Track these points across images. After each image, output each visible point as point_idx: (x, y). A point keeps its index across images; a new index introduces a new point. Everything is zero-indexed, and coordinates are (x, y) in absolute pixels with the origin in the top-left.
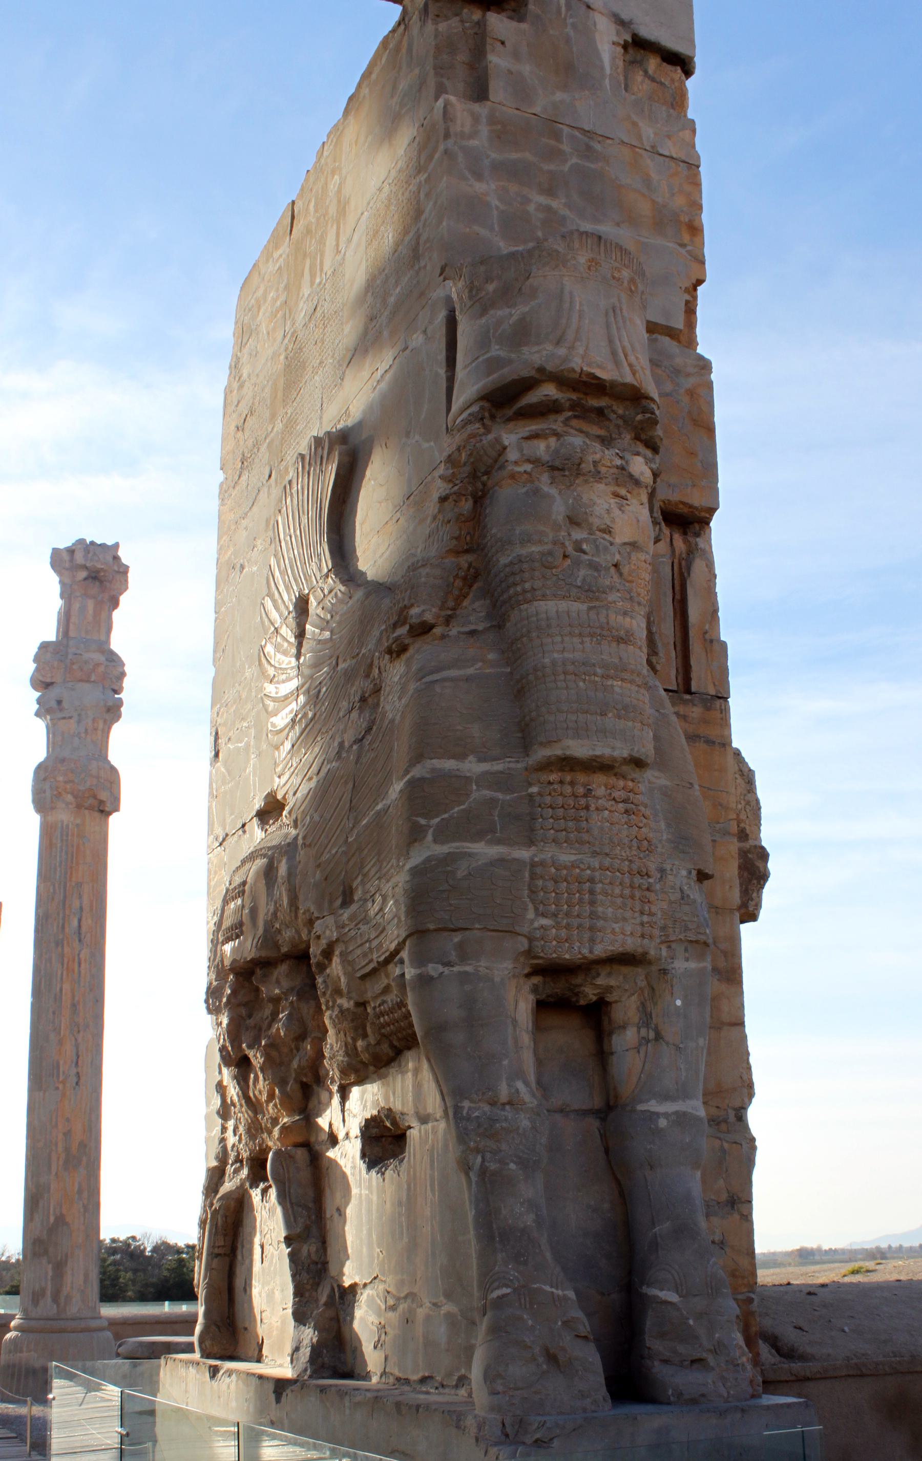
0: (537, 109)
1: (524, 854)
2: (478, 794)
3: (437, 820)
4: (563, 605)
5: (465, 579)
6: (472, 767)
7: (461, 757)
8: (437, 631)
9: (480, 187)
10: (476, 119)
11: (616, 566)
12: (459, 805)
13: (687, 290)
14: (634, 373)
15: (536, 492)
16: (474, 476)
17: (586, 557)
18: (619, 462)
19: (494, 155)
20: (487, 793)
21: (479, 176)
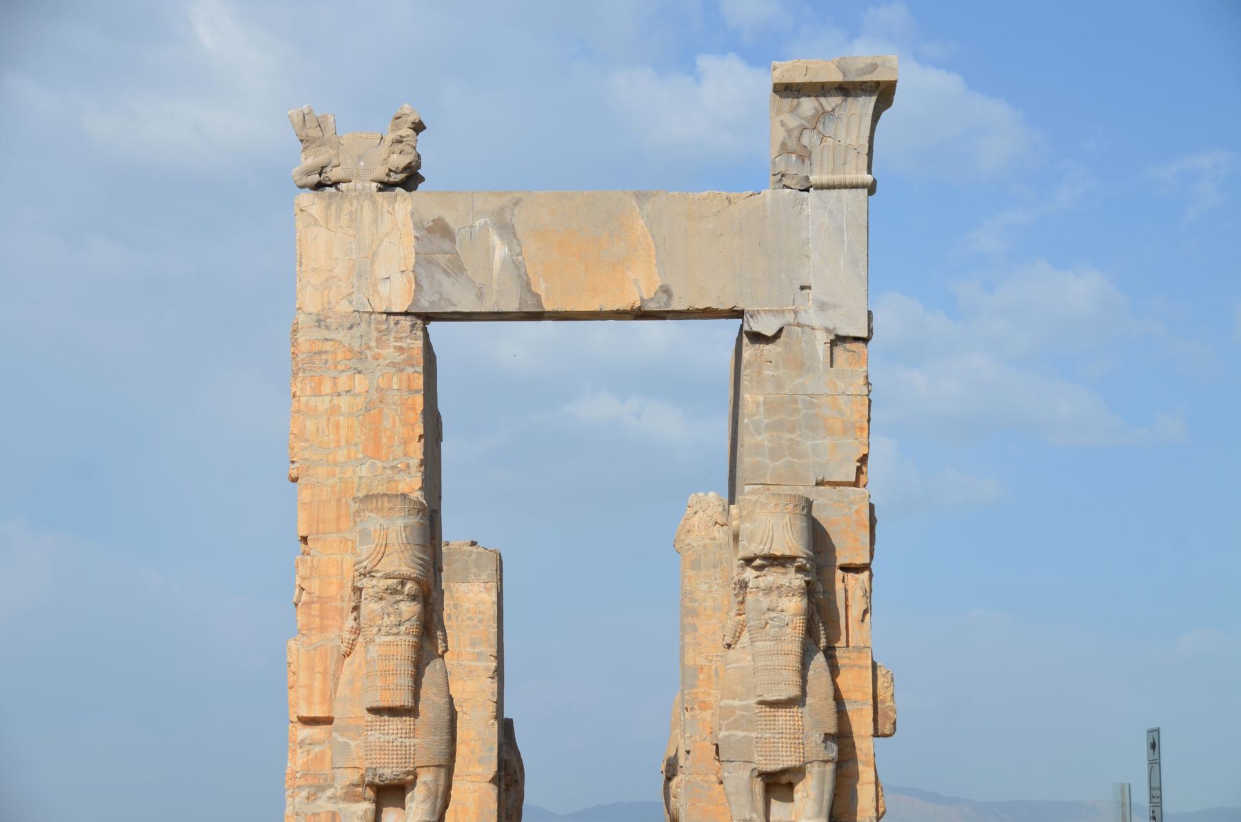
0: (787, 391)
1: (754, 735)
2: (738, 713)
3: (725, 723)
4: (765, 643)
5: (742, 625)
6: (737, 703)
7: (734, 699)
8: (732, 646)
9: (759, 438)
10: (758, 404)
11: (787, 624)
13: (858, 461)
14: (791, 550)
15: (757, 600)
16: (741, 587)
17: (776, 623)
18: (787, 584)
19: (766, 421)
20: (742, 713)
21: (759, 433)
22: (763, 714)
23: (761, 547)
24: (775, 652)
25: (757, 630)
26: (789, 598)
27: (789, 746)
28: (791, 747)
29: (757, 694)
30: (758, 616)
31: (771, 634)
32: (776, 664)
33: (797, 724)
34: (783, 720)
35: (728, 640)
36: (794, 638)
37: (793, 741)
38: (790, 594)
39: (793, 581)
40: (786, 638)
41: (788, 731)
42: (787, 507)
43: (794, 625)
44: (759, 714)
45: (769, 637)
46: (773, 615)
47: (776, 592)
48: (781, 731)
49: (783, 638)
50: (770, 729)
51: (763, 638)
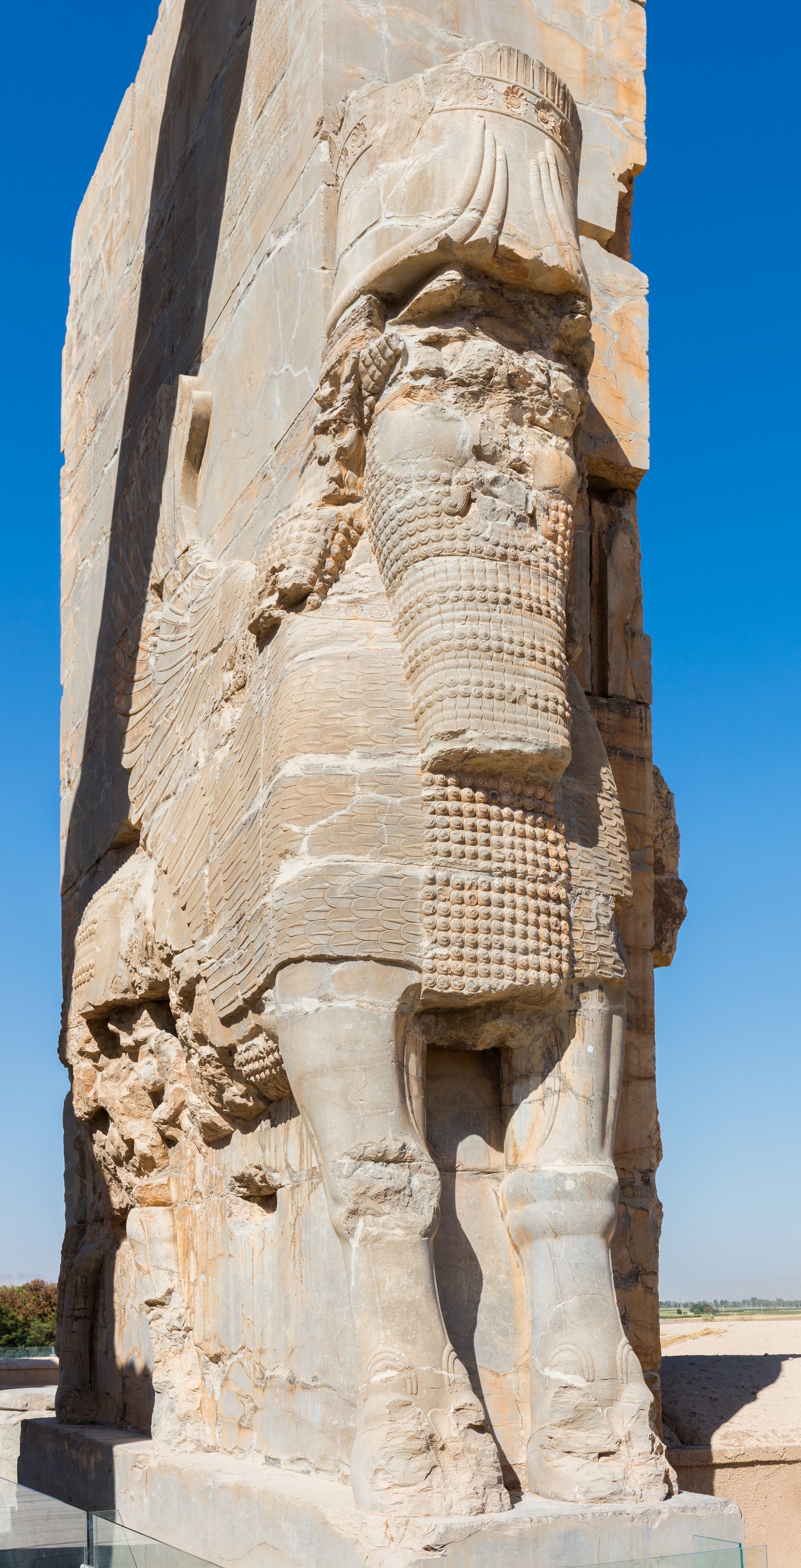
12: (339, 810)
16: (357, 398)
18: (540, 378)
20: (372, 795)
22: (452, 805)
23: (469, 216)
24: (502, 596)
25: (438, 514)
26: (537, 429)
27: (532, 916)
28: (537, 925)
29: (440, 729)
30: (443, 468)
31: (486, 534)
32: (505, 635)
33: (553, 852)
34: (514, 834)
35: (287, 580)
36: (551, 567)
37: (542, 904)
38: (545, 419)
39: (554, 374)
40: (532, 558)
41: (529, 868)
42: (541, 113)
43: (550, 524)
44: (439, 805)
45: (481, 543)
46: (489, 473)
47: (504, 396)
48: (508, 866)
49: (521, 554)
50: (475, 856)
51: (459, 545)
